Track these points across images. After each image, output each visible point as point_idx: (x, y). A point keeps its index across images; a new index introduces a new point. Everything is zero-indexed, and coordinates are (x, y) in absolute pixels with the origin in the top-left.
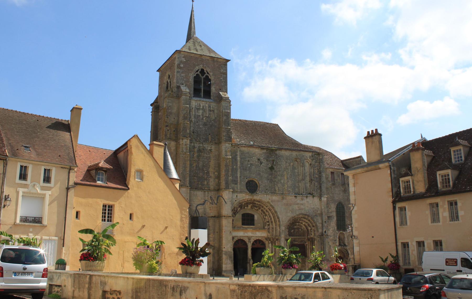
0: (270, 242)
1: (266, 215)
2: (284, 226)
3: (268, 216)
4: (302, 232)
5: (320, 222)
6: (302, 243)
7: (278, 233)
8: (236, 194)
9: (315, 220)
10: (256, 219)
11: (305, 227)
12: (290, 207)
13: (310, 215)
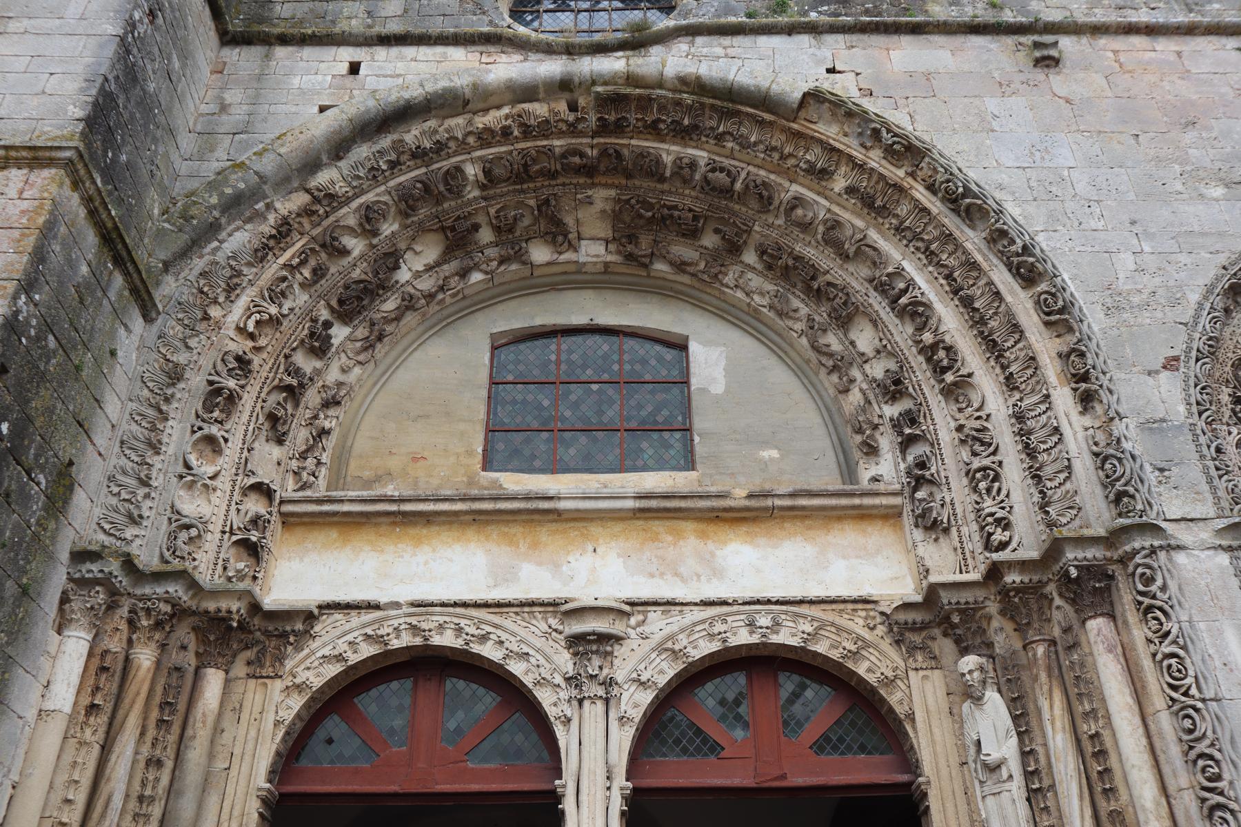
0: (970, 662)
1: (845, 315)
2: (1171, 364)
3: (878, 304)
7: (1084, 467)
8: (348, 54)
10: (718, 388)
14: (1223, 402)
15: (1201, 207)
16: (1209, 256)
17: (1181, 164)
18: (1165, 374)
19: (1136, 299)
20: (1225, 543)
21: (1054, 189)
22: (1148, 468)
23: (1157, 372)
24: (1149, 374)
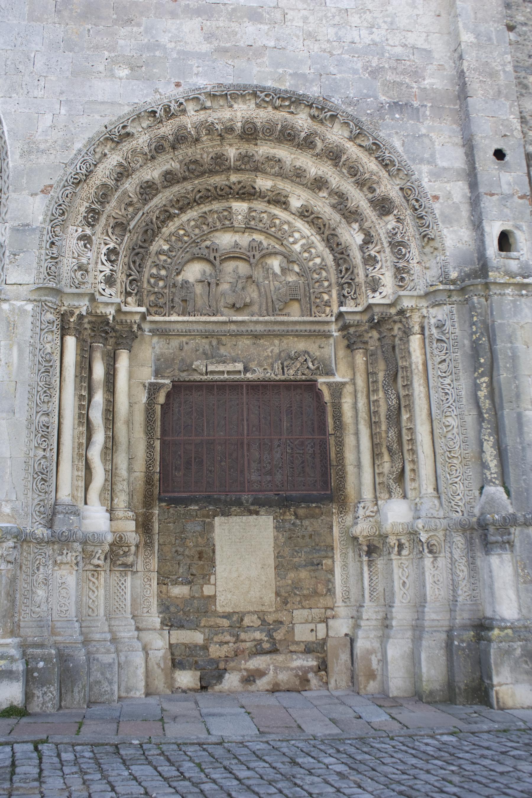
4: (291, 278)
5: (442, 163)
6: (290, 374)
9: (397, 144)
11: (316, 239)
12: (123, 31)
13: (336, 100)
14: (81, 212)
15: (109, 83)
16: (99, 118)
17: (109, 52)
18: (41, 195)
19: (42, 146)
20: (33, 298)
21: (21, 67)
22: (7, 253)
23: (36, 194)
24: (32, 195)
